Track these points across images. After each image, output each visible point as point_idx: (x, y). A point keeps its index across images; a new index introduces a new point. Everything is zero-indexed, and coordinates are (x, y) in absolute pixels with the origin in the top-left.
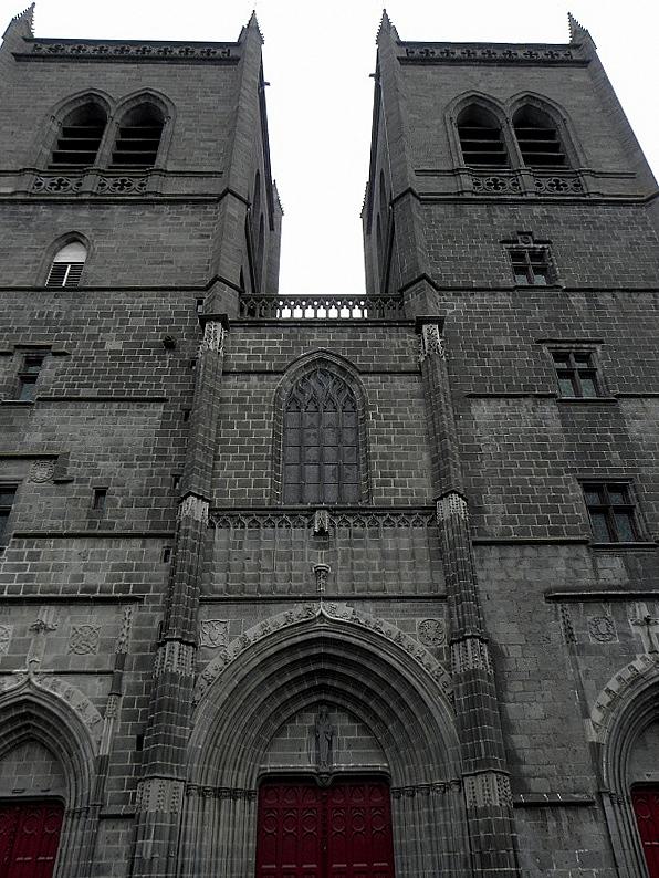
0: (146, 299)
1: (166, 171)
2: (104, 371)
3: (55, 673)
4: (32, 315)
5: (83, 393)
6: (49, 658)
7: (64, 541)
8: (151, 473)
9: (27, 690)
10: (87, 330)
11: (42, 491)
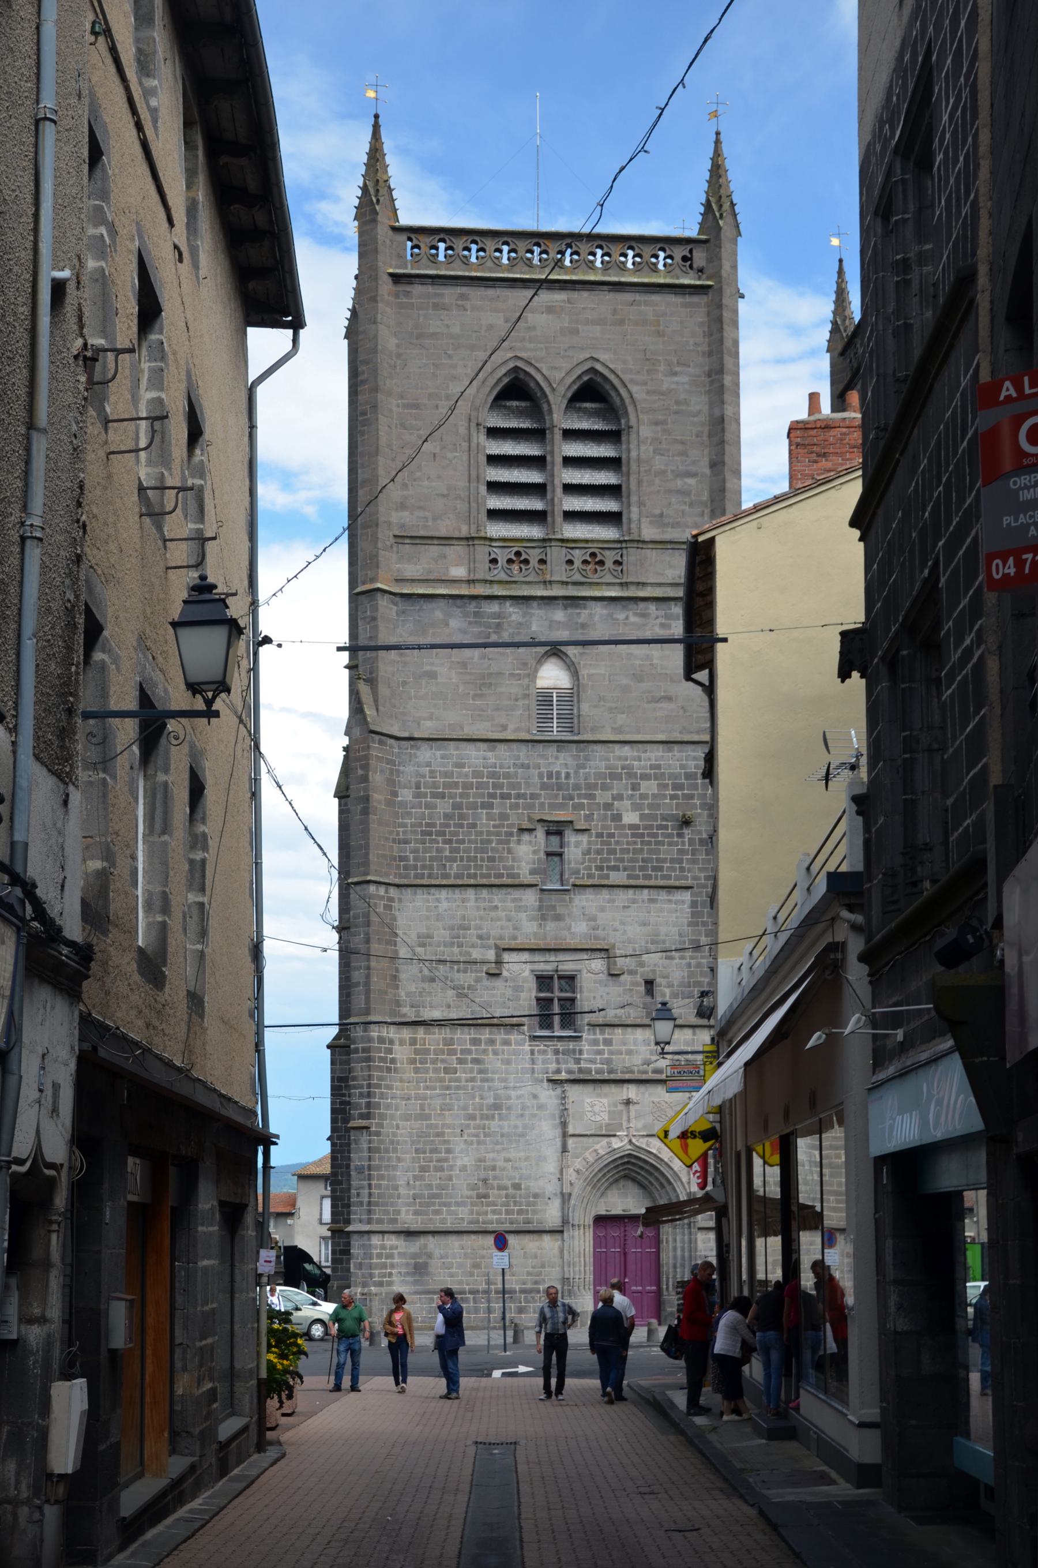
0: (655, 754)
1: (644, 542)
2: (628, 851)
3: (648, 1136)
4: (541, 776)
5: (617, 877)
6: (640, 1124)
7: (629, 1030)
8: (689, 965)
9: (629, 1147)
10: (602, 797)
11: (600, 982)
